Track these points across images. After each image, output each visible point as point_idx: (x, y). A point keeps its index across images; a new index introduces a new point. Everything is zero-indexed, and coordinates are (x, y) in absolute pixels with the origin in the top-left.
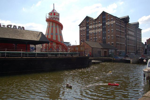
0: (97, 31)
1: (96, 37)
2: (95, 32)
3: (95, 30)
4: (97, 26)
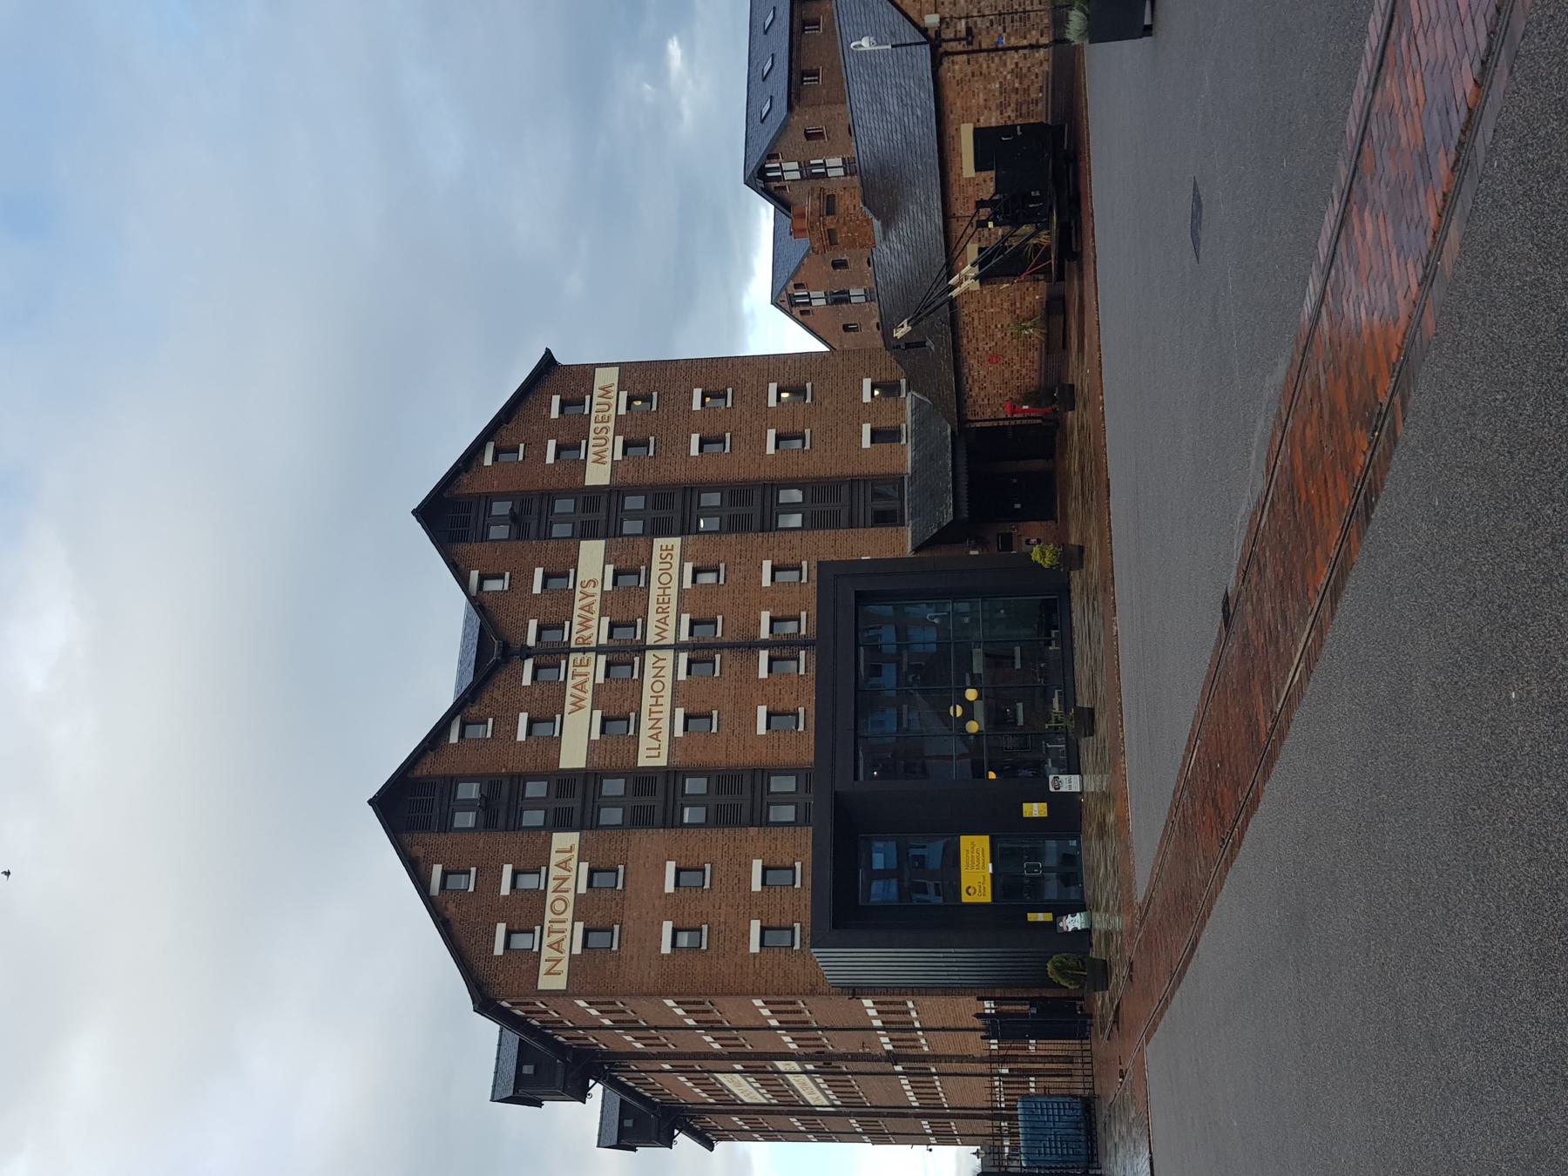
0: (664, 621)
1: (765, 633)
2: (678, 647)
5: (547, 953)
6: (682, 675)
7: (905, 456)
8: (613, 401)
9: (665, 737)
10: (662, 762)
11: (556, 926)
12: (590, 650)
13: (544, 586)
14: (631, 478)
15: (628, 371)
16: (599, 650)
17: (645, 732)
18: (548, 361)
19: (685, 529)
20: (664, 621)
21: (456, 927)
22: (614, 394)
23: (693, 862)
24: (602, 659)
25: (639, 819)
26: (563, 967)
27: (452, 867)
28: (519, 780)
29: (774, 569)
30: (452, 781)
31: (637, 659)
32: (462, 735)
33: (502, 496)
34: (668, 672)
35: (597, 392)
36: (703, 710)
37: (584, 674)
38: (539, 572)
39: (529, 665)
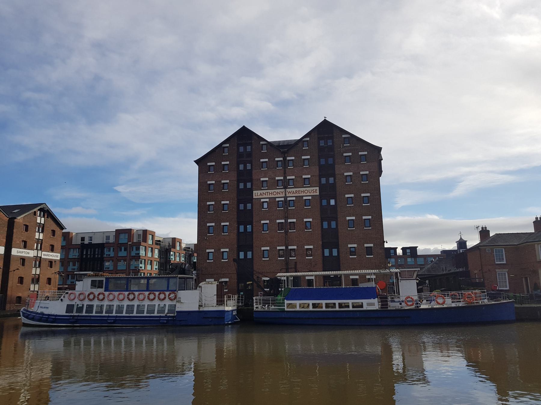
2: (286, 197)
3: (285, 188)
9: (261, 197)
17: (262, 192)
34: (279, 196)
39: (281, 159)
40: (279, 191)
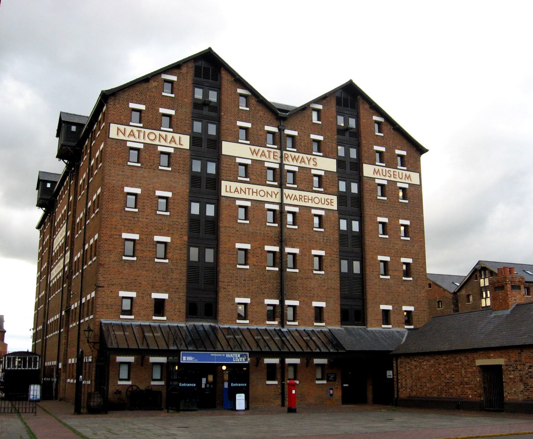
0: (295, 198)
2: (281, 205)
4: (294, 161)
5: (129, 129)
6: (267, 206)
7: (376, 327)
8: (403, 181)
9: (236, 195)
10: (223, 193)
11: (142, 134)
12: (282, 160)
13: (314, 141)
14: (366, 187)
15: (417, 189)
16: (281, 165)
18: (421, 150)
19: (342, 213)
20: (295, 198)
21: (145, 85)
22: (407, 181)
23: (171, 206)
24: (277, 166)
25: (195, 180)
26: (121, 137)
27: (175, 85)
28: (218, 121)
29: (320, 257)
30: (218, 89)
31: (276, 184)
32: (241, 95)
33: (358, 123)
35: (408, 173)
36: (249, 216)
37: (270, 157)
38: (321, 138)
39: (275, 130)
40: (270, 190)
